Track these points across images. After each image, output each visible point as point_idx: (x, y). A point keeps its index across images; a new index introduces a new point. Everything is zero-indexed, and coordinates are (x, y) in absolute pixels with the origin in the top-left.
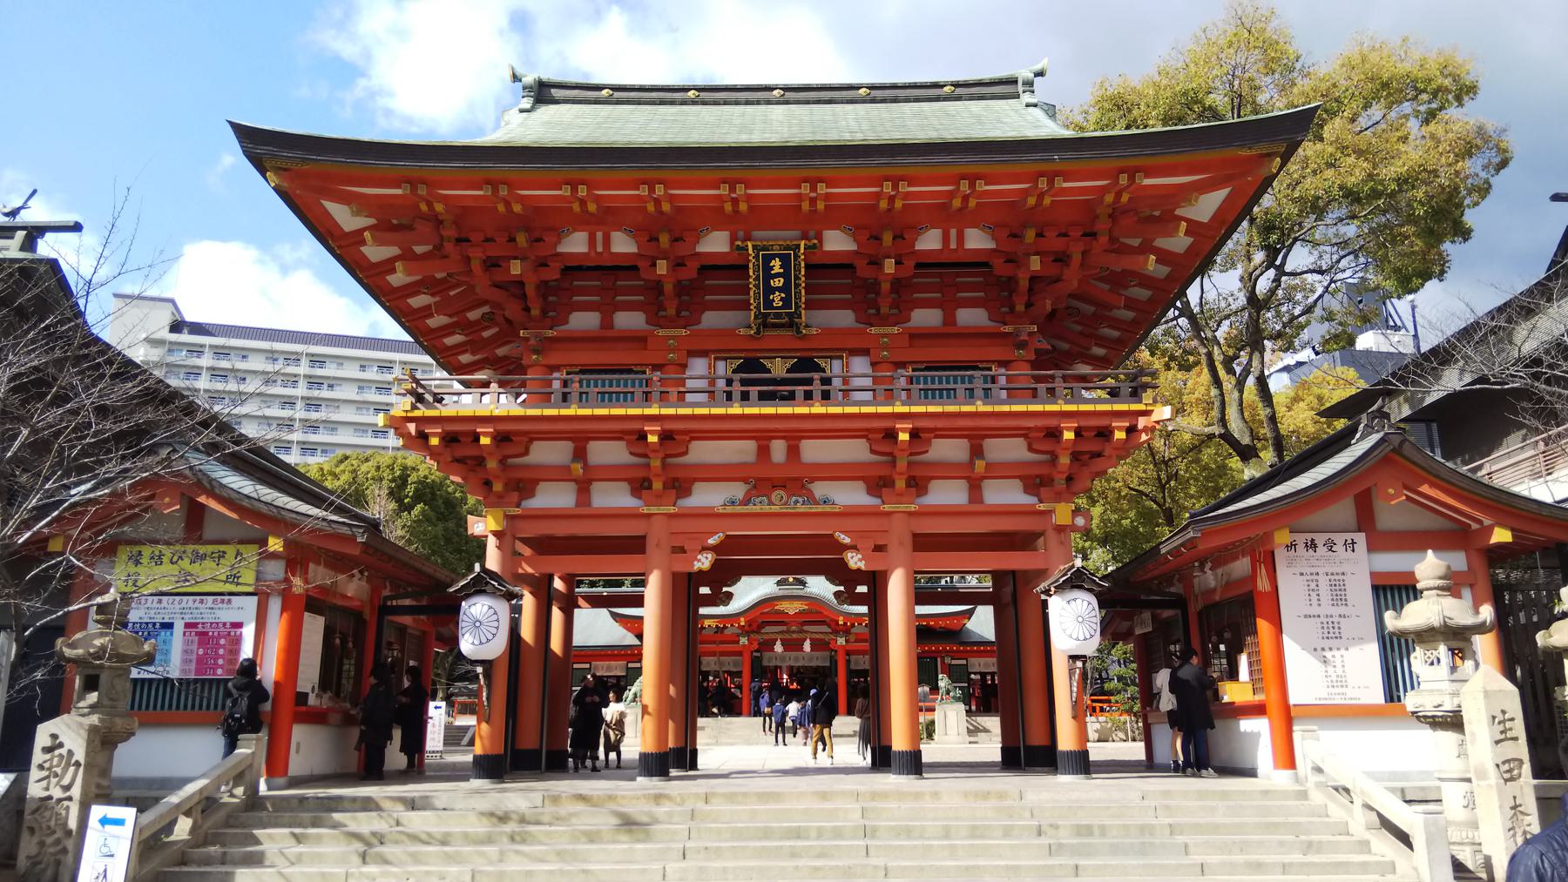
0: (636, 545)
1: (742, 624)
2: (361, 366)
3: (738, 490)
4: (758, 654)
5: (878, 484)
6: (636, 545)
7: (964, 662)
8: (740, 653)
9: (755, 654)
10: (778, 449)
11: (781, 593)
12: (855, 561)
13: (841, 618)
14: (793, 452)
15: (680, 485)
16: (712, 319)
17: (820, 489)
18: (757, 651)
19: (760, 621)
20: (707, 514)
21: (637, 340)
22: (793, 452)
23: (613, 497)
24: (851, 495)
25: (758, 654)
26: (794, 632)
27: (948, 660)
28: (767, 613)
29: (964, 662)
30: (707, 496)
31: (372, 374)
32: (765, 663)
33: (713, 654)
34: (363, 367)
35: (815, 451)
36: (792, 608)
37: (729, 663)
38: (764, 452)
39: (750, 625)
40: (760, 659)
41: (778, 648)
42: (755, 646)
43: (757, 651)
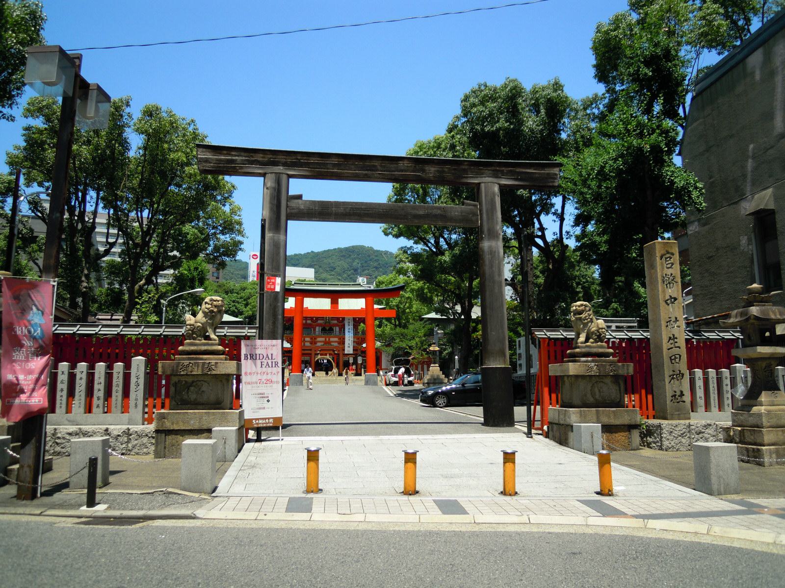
0: (311, 350)
3: (323, 344)
5: (339, 343)
6: (311, 350)
10: (327, 339)
12: (336, 352)
14: (329, 339)
15: (315, 343)
16: (319, 322)
17: (332, 344)
20: (319, 347)
21: (310, 325)
22: (329, 339)
23: (308, 344)
24: (336, 344)
30: (319, 344)
35: (332, 339)
38: (326, 339)
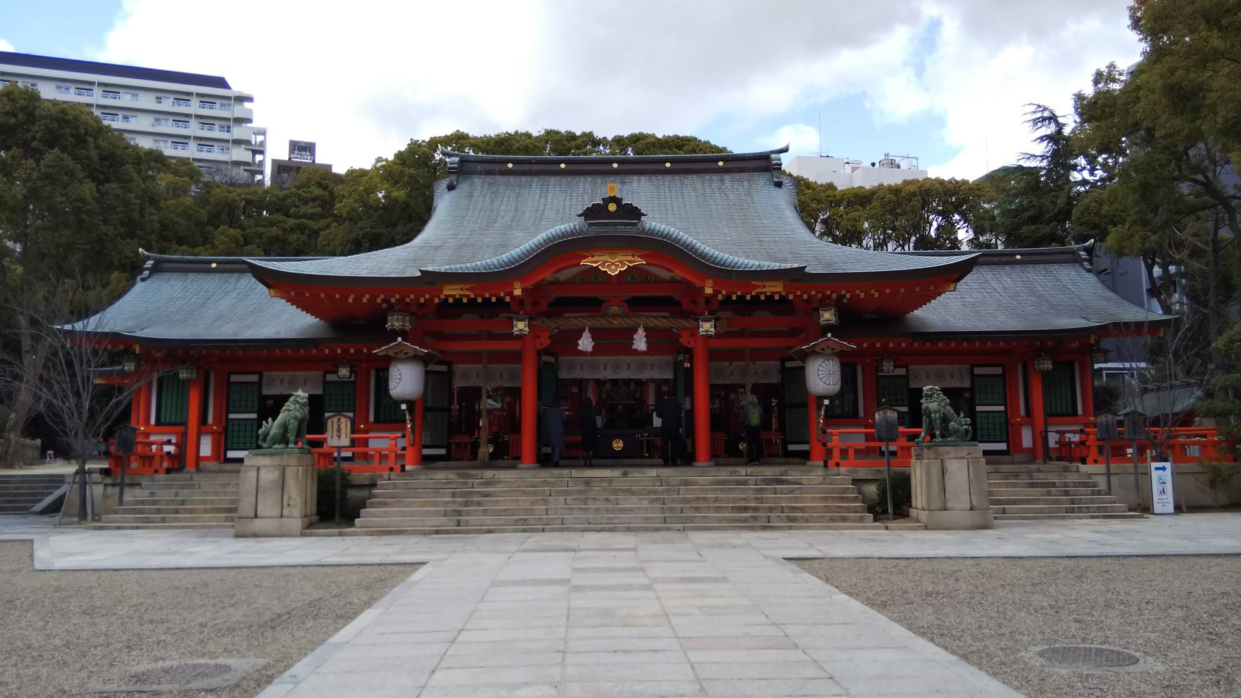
1: (518, 292)
2: (157, 98)
4: (551, 359)
7: (901, 372)
8: (516, 357)
9: (546, 358)
11: (594, 231)
13: (709, 283)
18: (547, 352)
19: (554, 296)
25: (551, 359)
26: (615, 316)
27: (888, 367)
28: (565, 282)
29: (901, 372)
31: (167, 105)
32: (564, 375)
33: (475, 357)
34: (159, 100)
36: (614, 265)
37: (502, 375)
39: (535, 304)
40: (554, 367)
41: (586, 343)
42: (545, 342)
43: (547, 352)
